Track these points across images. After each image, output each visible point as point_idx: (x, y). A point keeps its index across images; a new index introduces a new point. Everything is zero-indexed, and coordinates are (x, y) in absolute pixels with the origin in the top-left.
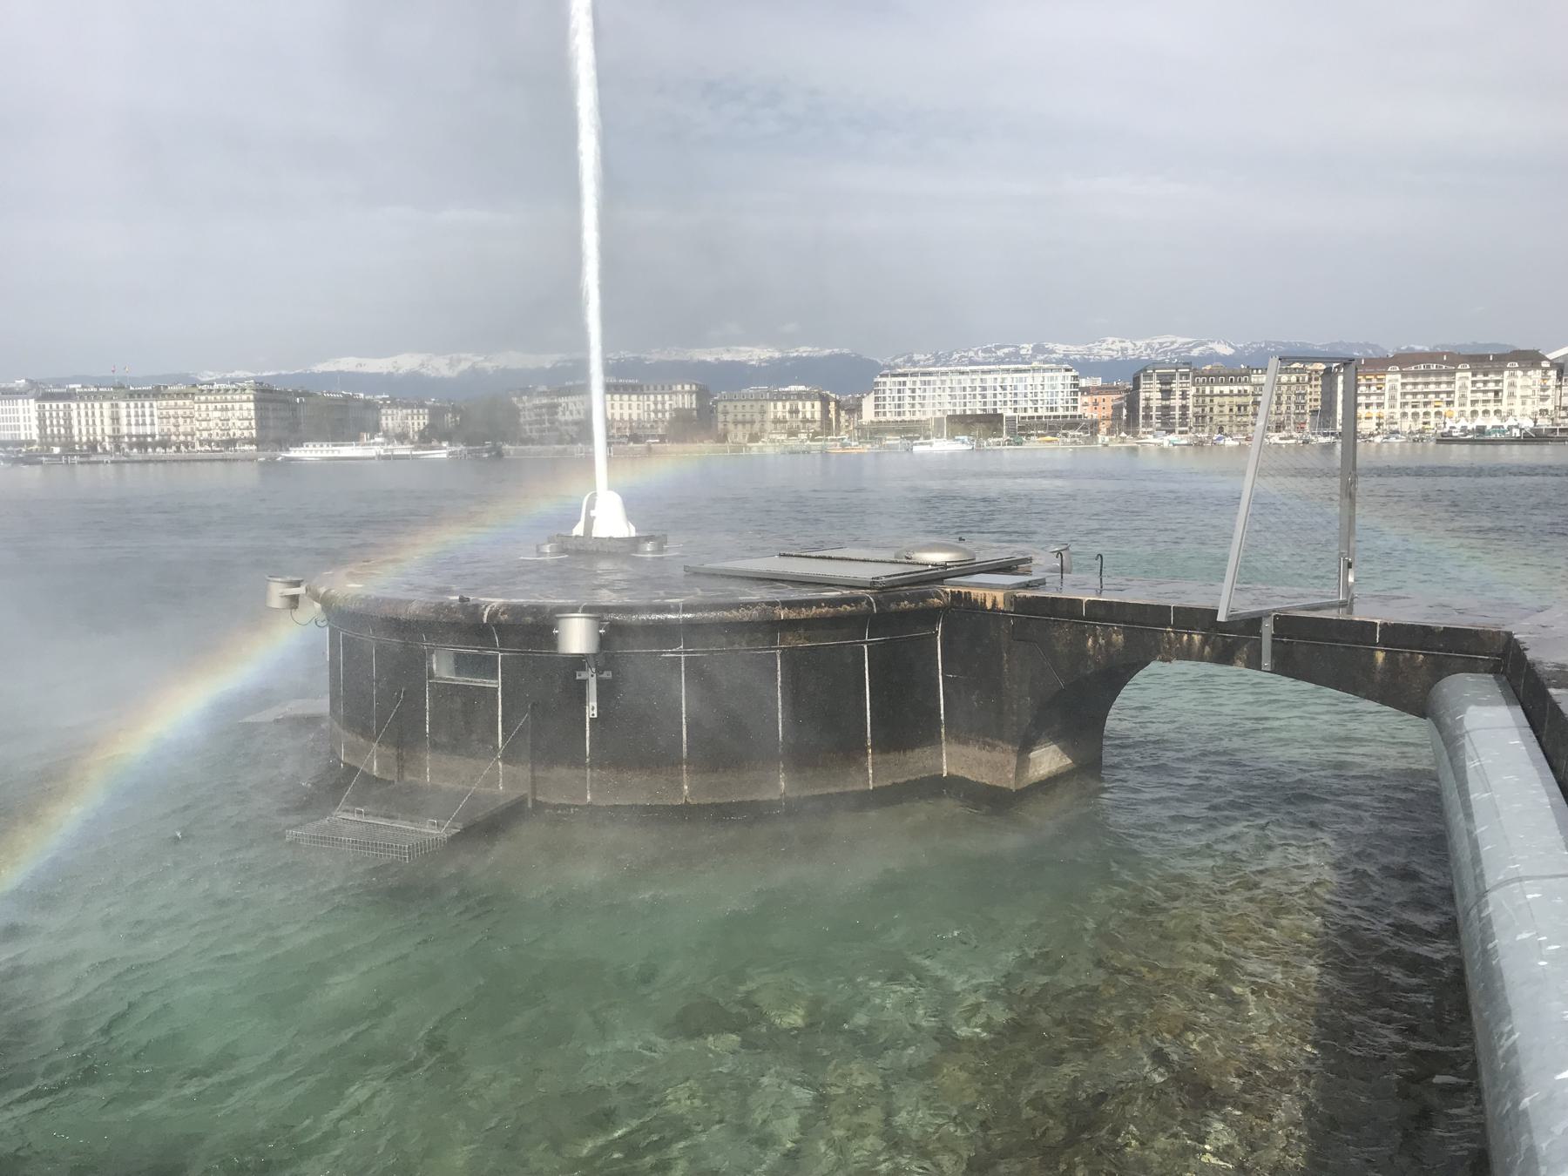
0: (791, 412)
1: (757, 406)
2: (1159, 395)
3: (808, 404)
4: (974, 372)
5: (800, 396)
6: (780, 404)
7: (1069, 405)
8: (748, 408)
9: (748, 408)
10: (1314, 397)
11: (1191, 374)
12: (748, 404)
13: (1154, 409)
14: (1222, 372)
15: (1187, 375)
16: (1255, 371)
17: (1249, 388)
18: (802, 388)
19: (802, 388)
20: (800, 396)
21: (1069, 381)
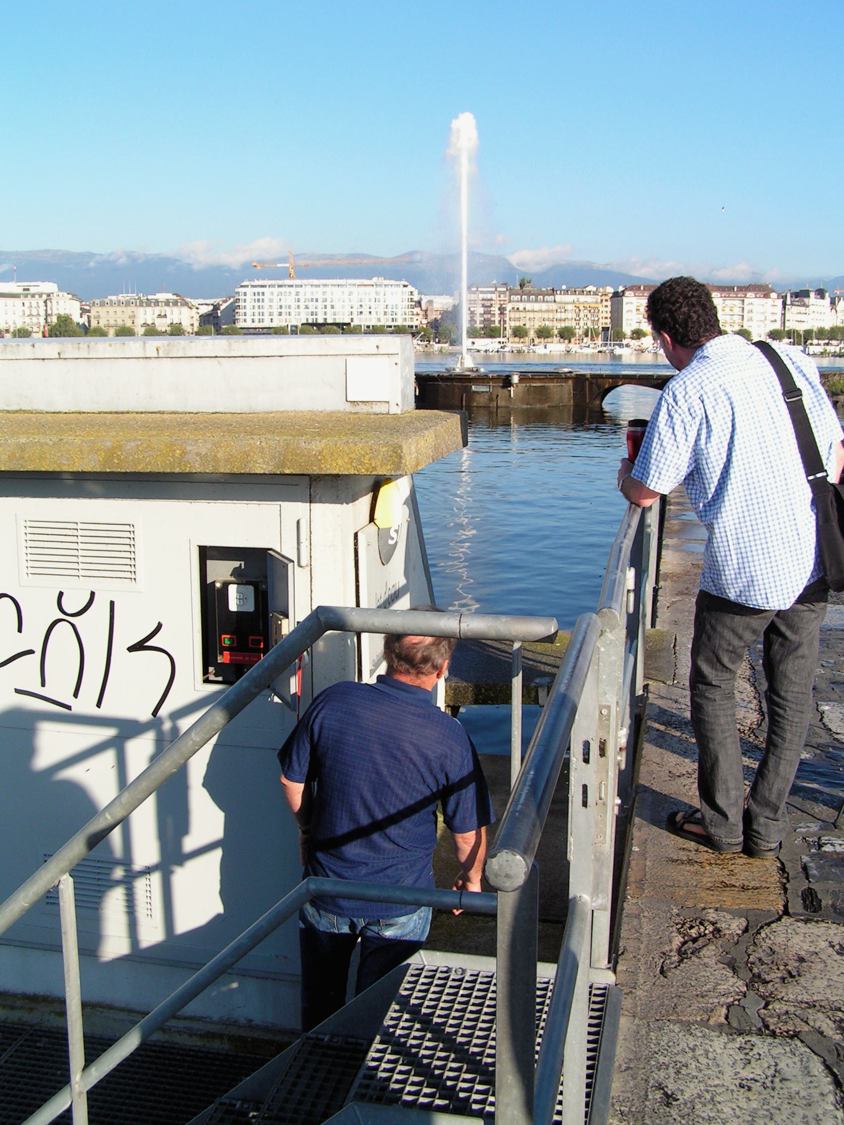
0: (160, 316)
1: (129, 310)
2: (481, 310)
3: (175, 309)
4: (273, 286)
5: (167, 303)
6: (149, 309)
7: (407, 317)
8: (119, 313)
9: (119, 313)
10: (605, 315)
11: (508, 293)
12: (119, 309)
13: (478, 322)
14: (532, 292)
15: (504, 293)
16: (558, 292)
17: (554, 306)
18: (170, 296)
19: (170, 296)
20: (167, 303)
21: (407, 296)
